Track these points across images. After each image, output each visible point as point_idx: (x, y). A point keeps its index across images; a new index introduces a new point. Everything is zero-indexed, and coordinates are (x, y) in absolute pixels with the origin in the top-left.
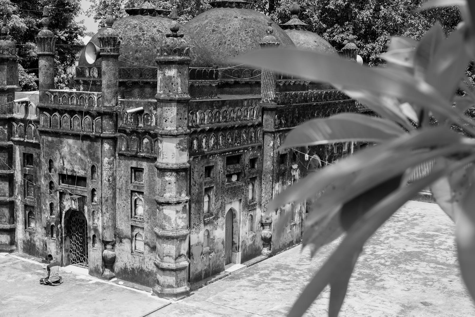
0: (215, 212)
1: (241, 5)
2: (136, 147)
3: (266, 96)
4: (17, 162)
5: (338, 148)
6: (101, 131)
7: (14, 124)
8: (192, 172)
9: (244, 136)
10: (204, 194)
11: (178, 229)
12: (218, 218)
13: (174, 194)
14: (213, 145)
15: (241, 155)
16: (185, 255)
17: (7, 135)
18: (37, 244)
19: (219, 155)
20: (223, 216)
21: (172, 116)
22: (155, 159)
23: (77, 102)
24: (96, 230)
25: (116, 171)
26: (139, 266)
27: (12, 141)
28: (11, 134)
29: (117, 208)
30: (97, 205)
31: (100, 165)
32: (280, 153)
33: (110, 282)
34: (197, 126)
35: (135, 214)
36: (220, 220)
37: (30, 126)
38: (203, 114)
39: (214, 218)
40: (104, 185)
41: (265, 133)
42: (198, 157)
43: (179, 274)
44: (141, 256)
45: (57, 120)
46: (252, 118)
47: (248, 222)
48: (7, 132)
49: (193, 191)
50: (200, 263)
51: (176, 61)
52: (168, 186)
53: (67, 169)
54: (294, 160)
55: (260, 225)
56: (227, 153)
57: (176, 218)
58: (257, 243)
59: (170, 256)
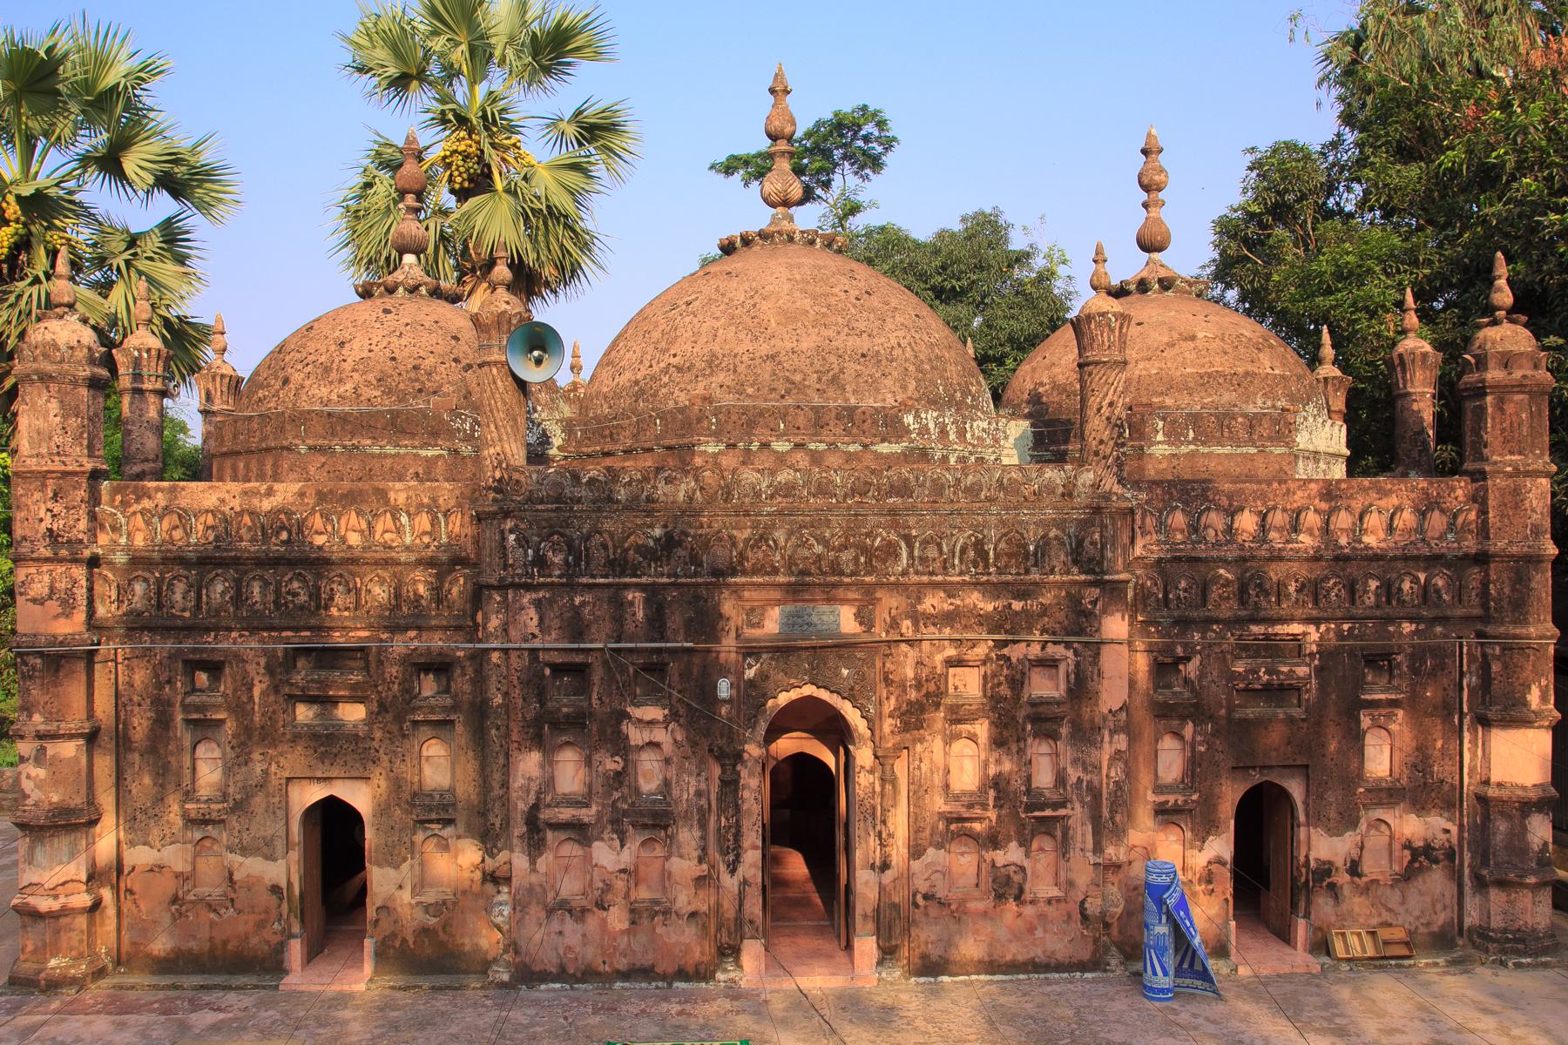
5: (985, 677)
19: (247, 633)
39: (233, 810)
56: (284, 634)
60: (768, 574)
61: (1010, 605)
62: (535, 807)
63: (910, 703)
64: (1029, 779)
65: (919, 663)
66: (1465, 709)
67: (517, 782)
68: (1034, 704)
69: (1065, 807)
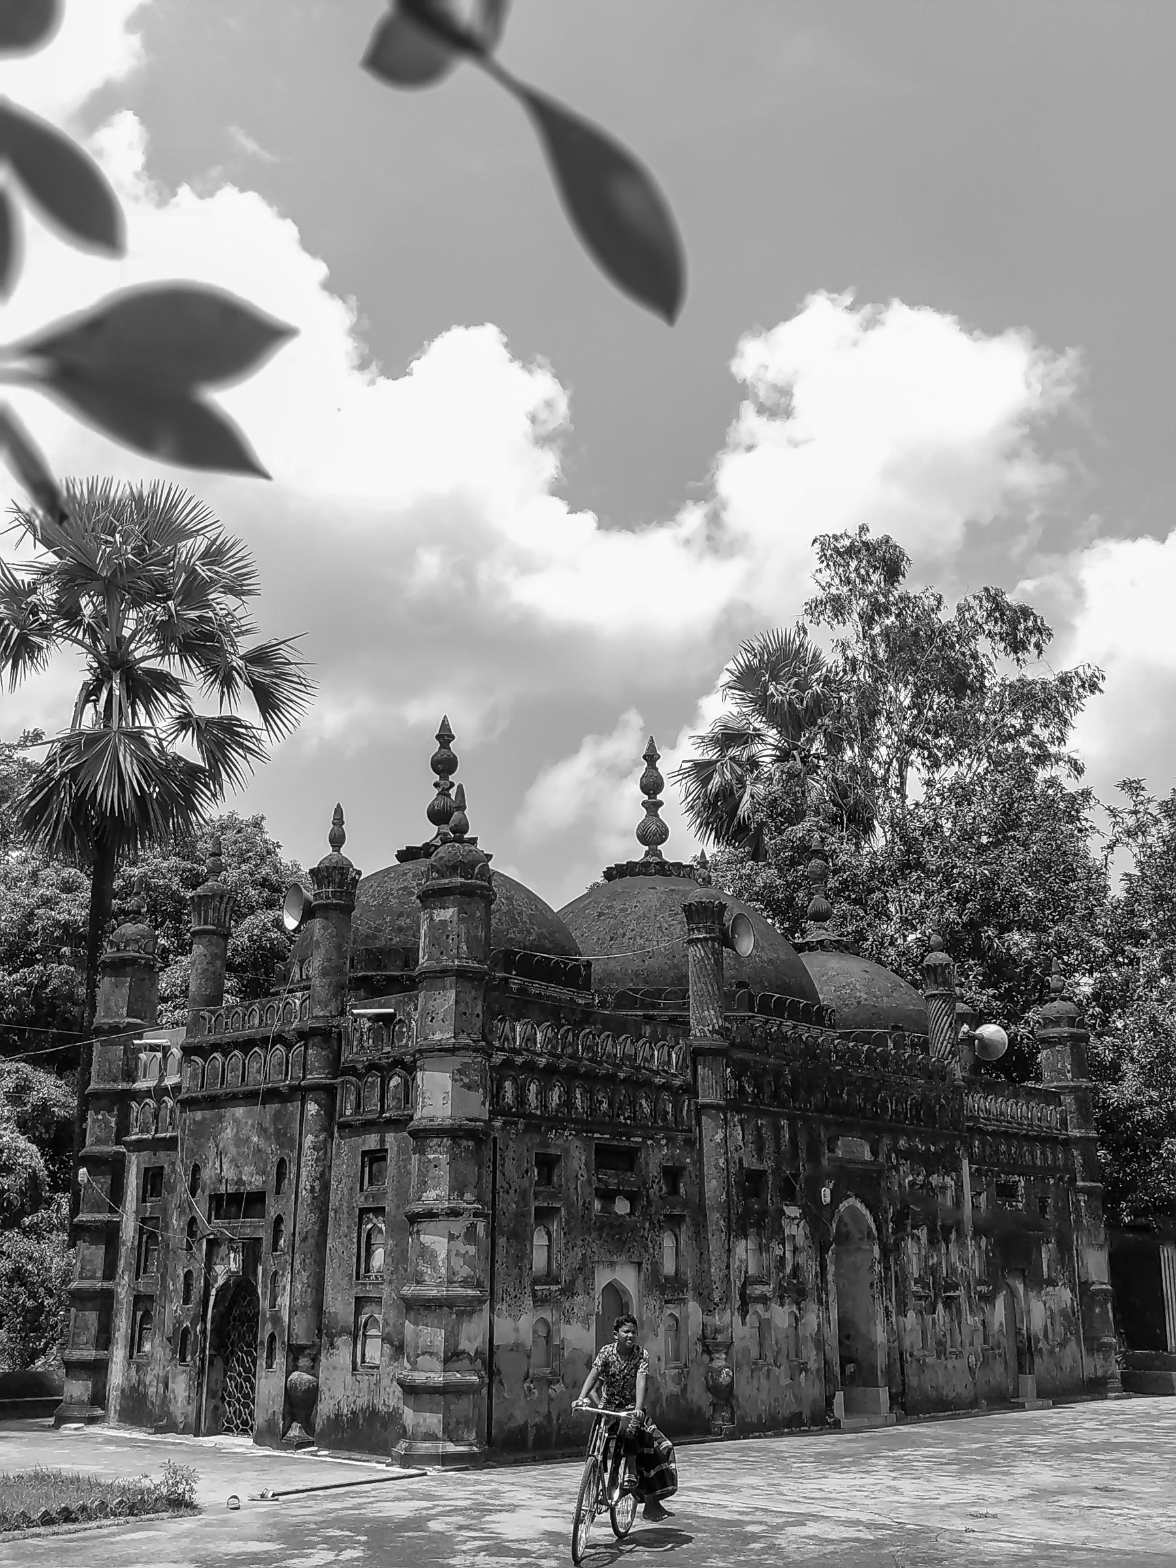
0: (565, 1276)
1: (669, 870)
2: (376, 1099)
3: (701, 1021)
4: (129, 1193)
6: (304, 1073)
7: (134, 1104)
9: (643, 1102)
10: (532, 1221)
11: (455, 1282)
12: (573, 1294)
13: (443, 1191)
14: (558, 1105)
15: (638, 1149)
16: (473, 1355)
17: (114, 1130)
18: (152, 1390)
19: (574, 1133)
20: (588, 1294)
21: (447, 1006)
22: (411, 1118)
23: (261, 1020)
24: (276, 1319)
25: (330, 1167)
26: (369, 1401)
27: (125, 1144)
28: (123, 1128)
29: (328, 1259)
30: (284, 1254)
31: (296, 1154)
32: (745, 1165)
33: (300, 1454)
34: (515, 1051)
35: (367, 1270)
36: (579, 1299)
37: (164, 1101)
38: (530, 1026)
39: (562, 1292)
40: (302, 1203)
41: (701, 1110)
42: (516, 1124)
43: (454, 1404)
44: (373, 1375)
45: (214, 1067)
46: (666, 1068)
47: (661, 1330)
48: (116, 1124)
49: (500, 1205)
51: (456, 887)
52: (433, 1172)
53: (227, 1180)
54: (788, 1194)
55: (699, 1348)
56: (595, 1135)
57: (449, 1251)
58: (695, 1399)
59: (431, 1354)
62: (744, 1286)
65: (900, 1185)
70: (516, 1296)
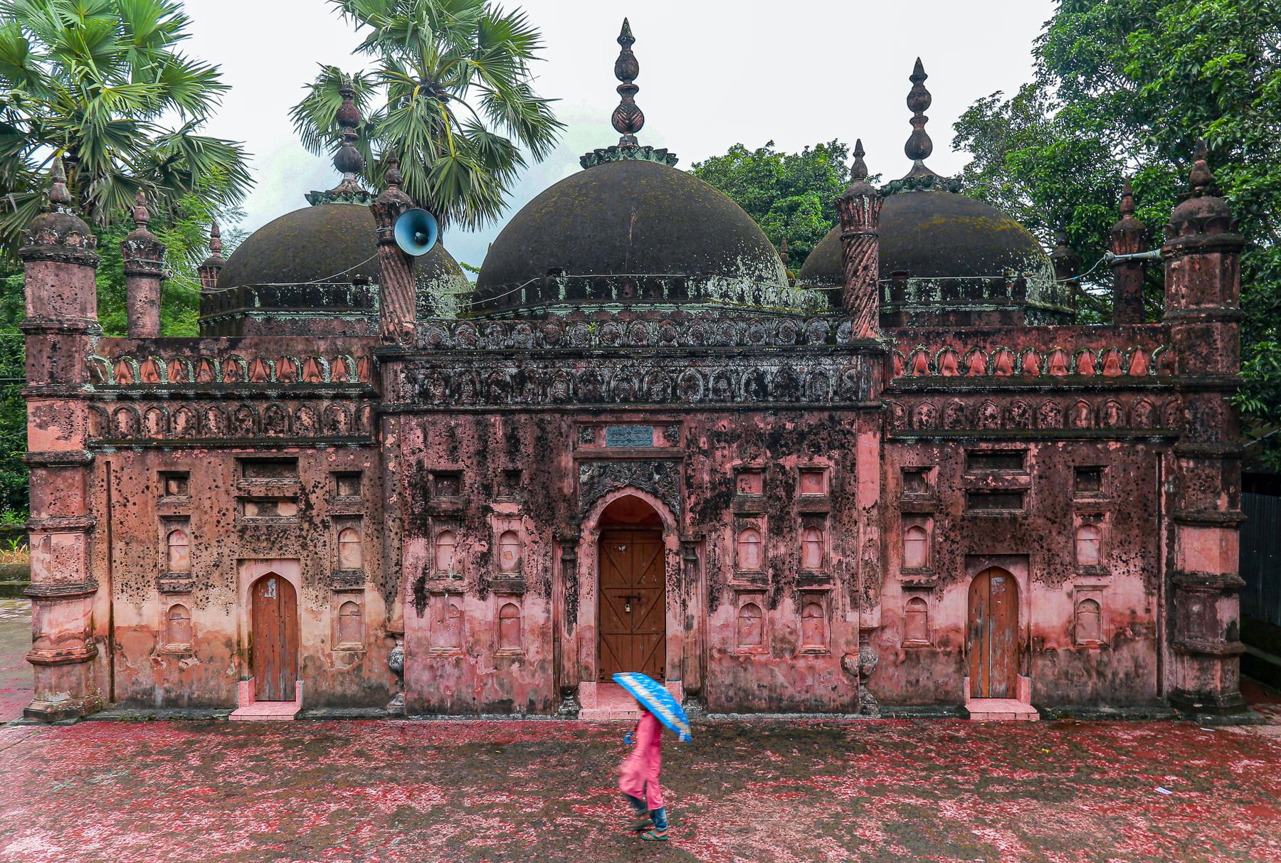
5: (765, 481)
8: (113, 478)
32: (428, 464)
50: (148, 671)
56: (234, 451)
60: (596, 401)
61: (785, 425)
62: (422, 581)
63: (706, 501)
64: (800, 561)
65: (713, 471)
66: (1164, 513)
67: (408, 561)
68: (807, 501)
69: (829, 583)
70: (138, 589)
